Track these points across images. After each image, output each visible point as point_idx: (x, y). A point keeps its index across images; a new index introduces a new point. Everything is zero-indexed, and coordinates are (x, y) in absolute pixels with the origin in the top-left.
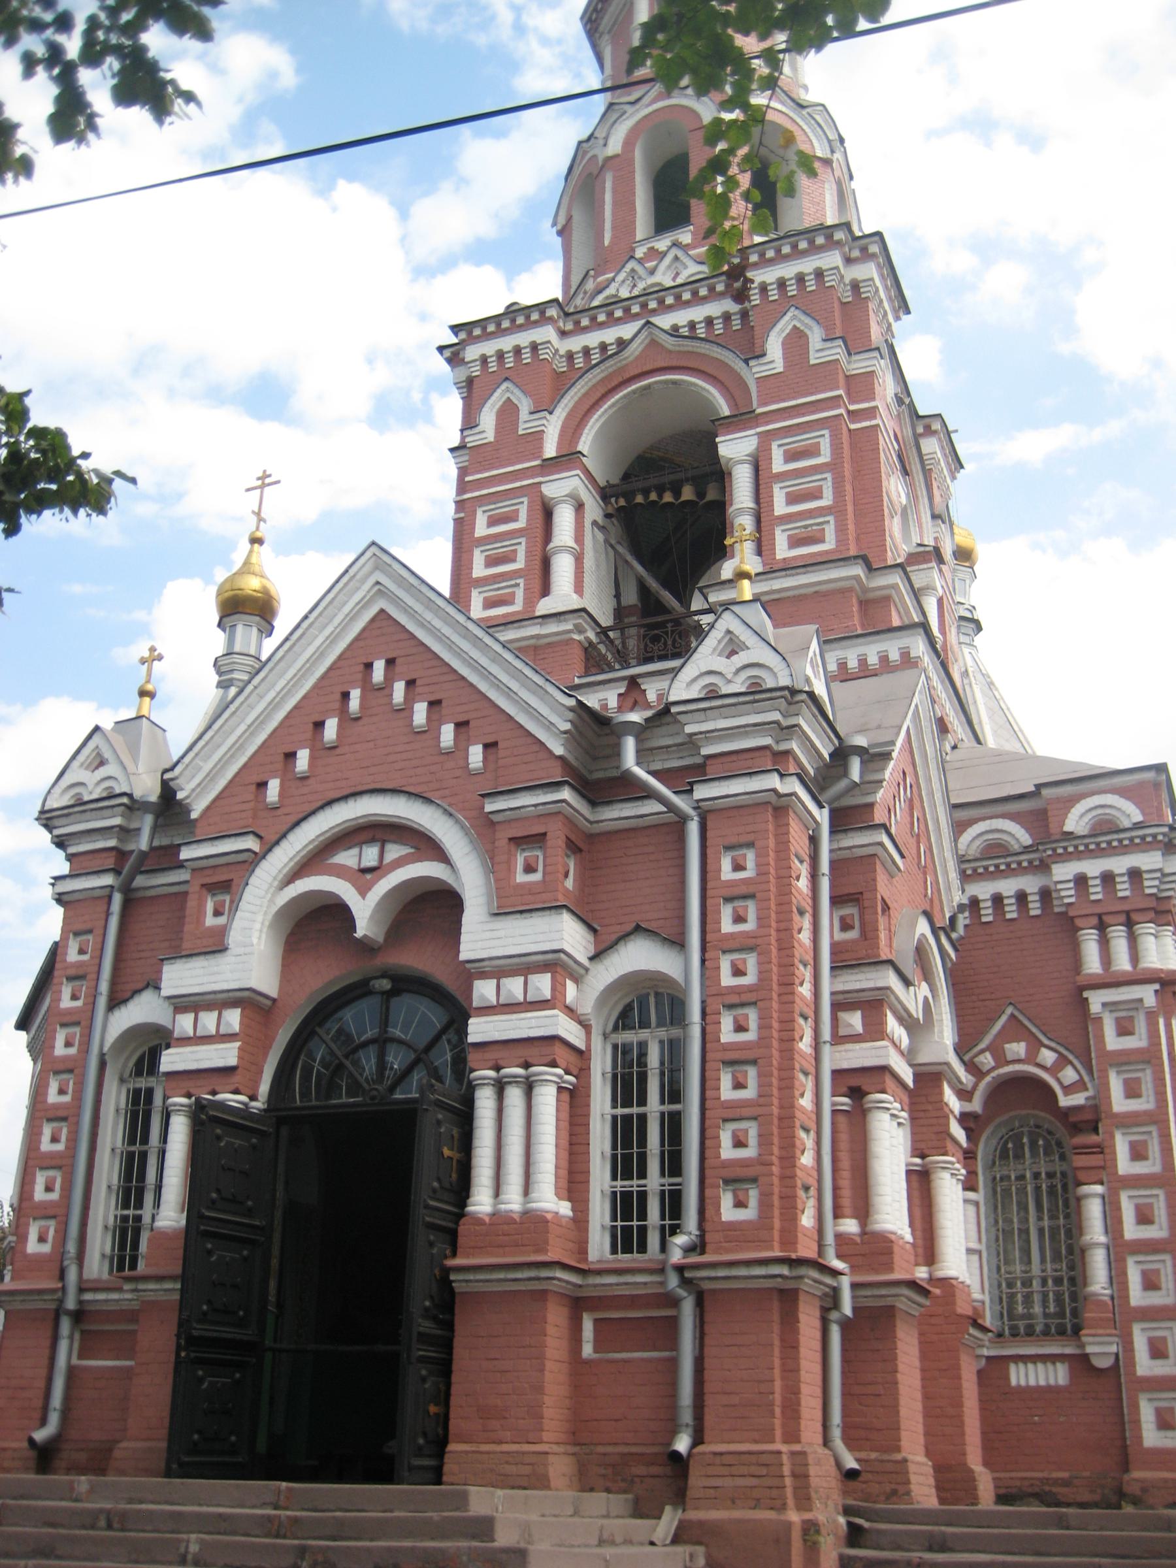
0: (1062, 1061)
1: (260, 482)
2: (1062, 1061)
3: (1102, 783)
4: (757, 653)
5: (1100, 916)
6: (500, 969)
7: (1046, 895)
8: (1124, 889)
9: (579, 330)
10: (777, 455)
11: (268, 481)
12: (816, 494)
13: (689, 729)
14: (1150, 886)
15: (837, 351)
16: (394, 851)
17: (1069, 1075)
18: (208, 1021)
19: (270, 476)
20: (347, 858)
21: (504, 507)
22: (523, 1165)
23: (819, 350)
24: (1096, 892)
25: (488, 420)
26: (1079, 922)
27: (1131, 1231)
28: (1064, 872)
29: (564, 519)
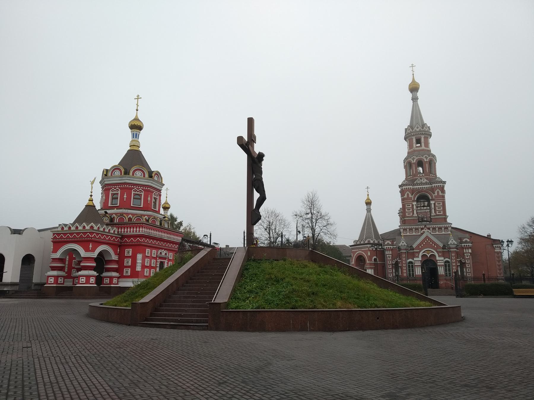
22: (441, 271)
23: (440, 194)
25: (406, 195)
28: (463, 245)
29: (415, 207)
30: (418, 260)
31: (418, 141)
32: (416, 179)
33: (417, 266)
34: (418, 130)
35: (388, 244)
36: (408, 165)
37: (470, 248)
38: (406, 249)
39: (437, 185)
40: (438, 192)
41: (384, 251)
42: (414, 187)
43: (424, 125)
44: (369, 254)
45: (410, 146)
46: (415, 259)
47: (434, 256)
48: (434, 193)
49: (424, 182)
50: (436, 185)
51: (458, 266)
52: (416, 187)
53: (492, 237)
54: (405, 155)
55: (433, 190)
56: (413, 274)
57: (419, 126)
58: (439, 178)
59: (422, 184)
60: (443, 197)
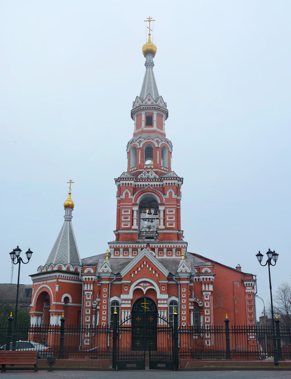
0: (200, 301)
1: (70, 182)
2: (200, 301)
3: (207, 266)
4: (186, 268)
5: (205, 283)
6: (161, 300)
7: (199, 279)
8: (208, 280)
9: (137, 181)
10: (167, 211)
11: (71, 182)
12: (172, 218)
13: (179, 275)
14: (211, 280)
15: (176, 197)
16: (148, 284)
17: (200, 302)
18: (126, 302)
19: (72, 181)
20: (142, 284)
21: (126, 210)
23: (174, 196)
24: (205, 280)
26: (203, 284)
27: (206, 321)
29: (135, 213)
30: (126, 299)
31: (149, 122)
32: (140, 173)
33: (125, 308)
34: (149, 103)
35: (89, 273)
36: (132, 148)
37: (212, 283)
38: (109, 279)
39: (170, 182)
40: (171, 193)
41: (81, 285)
42: (137, 183)
43: (159, 98)
44: (57, 289)
45: (138, 125)
46: (123, 296)
47: (152, 291)
48: (164, 194)
49: (153, 177)
50: (168, 182)
51: (190, 311)
52: (139, 183)
53: (243, 270)
54: (130, 137)
55: (163, 190)
56: (129, 327)
57: (151, 98)
58: (174, 173)
59: (148, 179)
60: (178, 201)
